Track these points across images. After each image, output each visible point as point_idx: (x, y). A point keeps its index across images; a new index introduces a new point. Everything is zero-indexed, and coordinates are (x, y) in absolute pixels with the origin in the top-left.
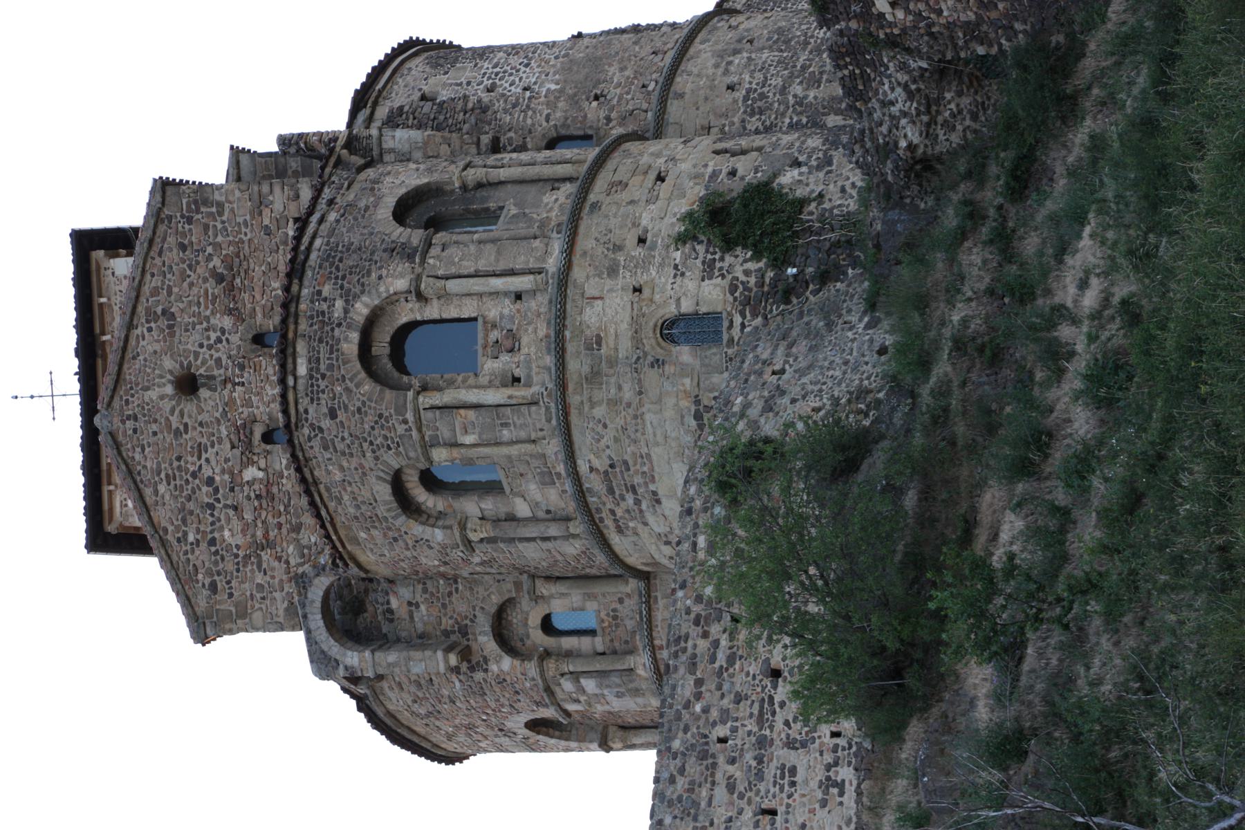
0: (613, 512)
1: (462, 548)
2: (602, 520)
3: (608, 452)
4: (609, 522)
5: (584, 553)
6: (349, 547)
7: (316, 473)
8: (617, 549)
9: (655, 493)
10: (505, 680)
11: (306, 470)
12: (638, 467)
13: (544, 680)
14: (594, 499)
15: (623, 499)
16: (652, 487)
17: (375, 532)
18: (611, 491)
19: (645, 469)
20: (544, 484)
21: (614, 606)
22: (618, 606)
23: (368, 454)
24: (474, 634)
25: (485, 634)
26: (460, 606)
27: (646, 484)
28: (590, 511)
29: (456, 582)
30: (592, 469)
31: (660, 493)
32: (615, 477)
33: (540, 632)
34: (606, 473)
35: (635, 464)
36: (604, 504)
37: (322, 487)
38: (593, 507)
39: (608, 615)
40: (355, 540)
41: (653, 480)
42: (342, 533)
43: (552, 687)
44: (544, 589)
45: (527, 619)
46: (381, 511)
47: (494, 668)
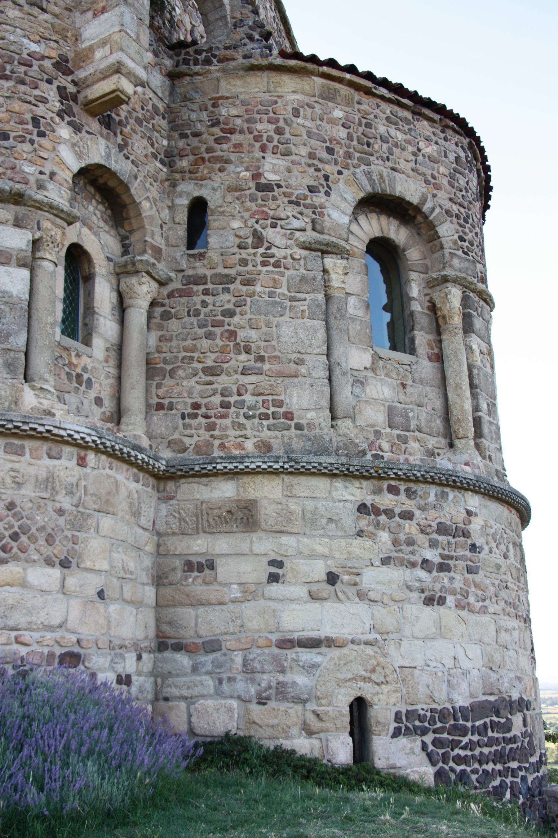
0: (407, 516)
1: (310, 236)
2: (393, 490)
3: (486, 548)
4: (386, 500)
5: (289, 416)
6: (319, 81)
7: (425, 123)
8: (321, 485)
9: (442, 601)
10: (42, 134)
11: (437, 117)
12: (473, 589)
13: (39, 206)
14: (432, 498)
15: (433, 544)
16: (450, 600)
17: (343, 133)
18: (442, 529)
19: (472, 599)
20: (391, 412)
21: (96, 386)
22: (93, 394)
23: (455, 208)
24: (107, 139)
25: (108, 156)
26: (139, 146)
27: (453, 592)
28: (417, 481)
29: (162, 162)
30: (469, 513)
31: (442, 610)
32: (462, 547)
33: (75, 240)
34: (466, 534)
35: (476, 585)
36: (423, 509)
37: (409, 115)
38: (420, 488)
39: (85, 369)
40: (328, 96)
41: (459, 606)
42: (344, 90)
43: (21, 210)
44: (144, 291)
45: (90, 228)
46: (378, 167)
47: (64, 132)
